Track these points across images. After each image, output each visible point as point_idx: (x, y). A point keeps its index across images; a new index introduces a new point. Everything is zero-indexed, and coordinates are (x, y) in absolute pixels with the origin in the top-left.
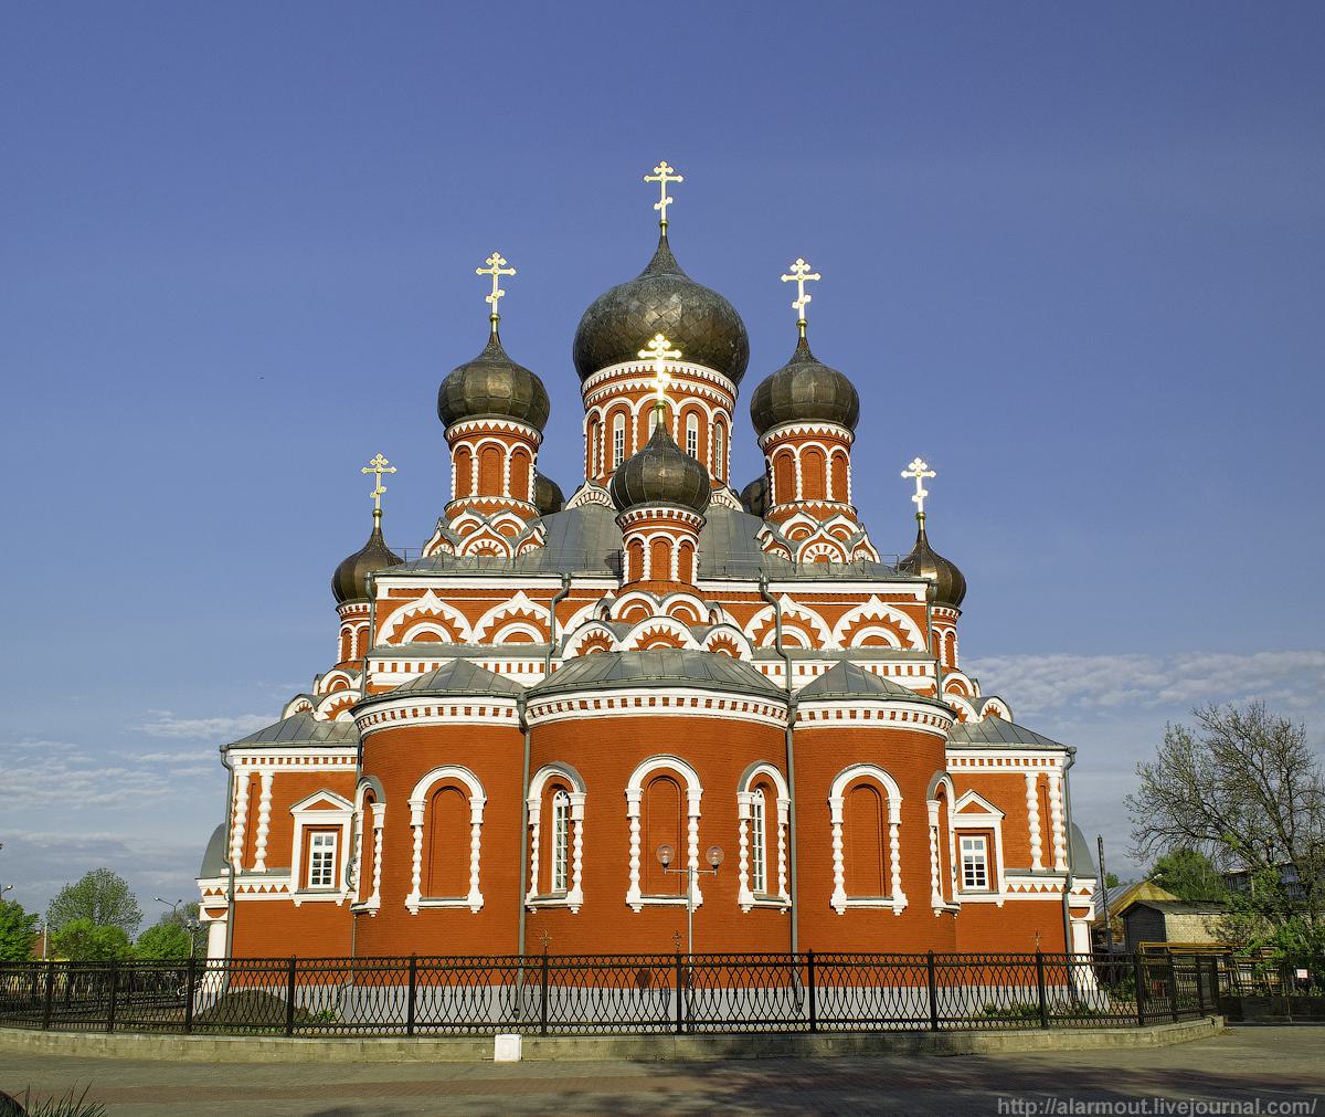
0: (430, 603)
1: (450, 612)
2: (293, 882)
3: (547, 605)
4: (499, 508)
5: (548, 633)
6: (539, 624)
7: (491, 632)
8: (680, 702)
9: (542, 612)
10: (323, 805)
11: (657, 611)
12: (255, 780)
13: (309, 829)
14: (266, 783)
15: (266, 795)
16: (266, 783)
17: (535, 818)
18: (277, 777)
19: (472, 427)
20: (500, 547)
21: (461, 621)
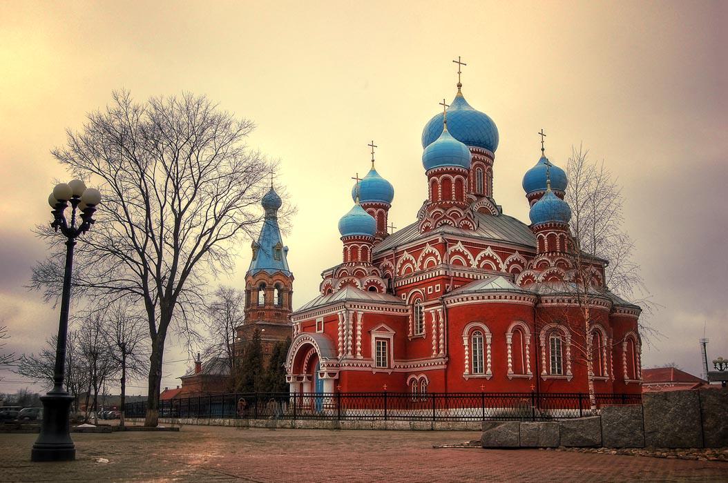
0: (459, 247)
1: (467, 252)
2: (374, 364)
3: (497, 253)
4: (451, 206)
5: (497, 264)
6: (495, 261)
7: (480, 262)
8: (552, 301)
9: (496, 256)
10: (383, 329)
11: (552, 264)
12: (355, 315)
13: (376, 338)
14: (360, 317)
15: (359, 322)
16: (360, 317)
17: (543, 344)
18: (365, 316)
19: (440, 170)
20: (471, 225)
21: (470, 257)
